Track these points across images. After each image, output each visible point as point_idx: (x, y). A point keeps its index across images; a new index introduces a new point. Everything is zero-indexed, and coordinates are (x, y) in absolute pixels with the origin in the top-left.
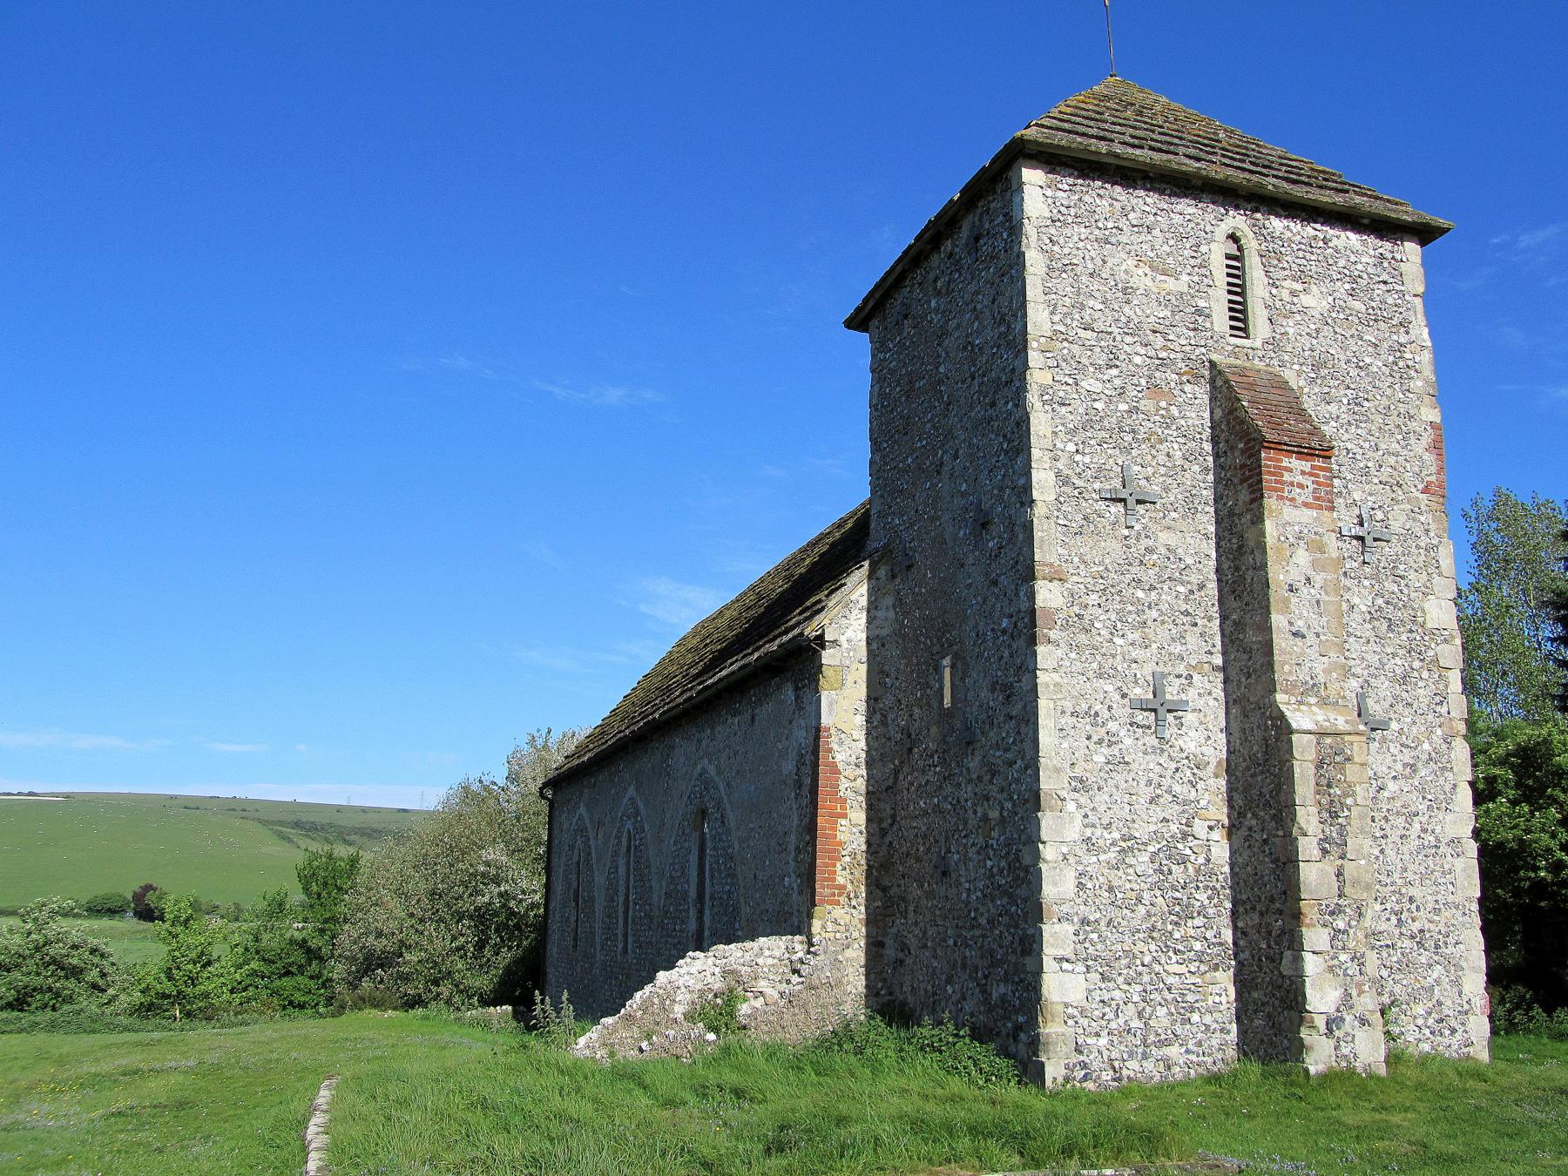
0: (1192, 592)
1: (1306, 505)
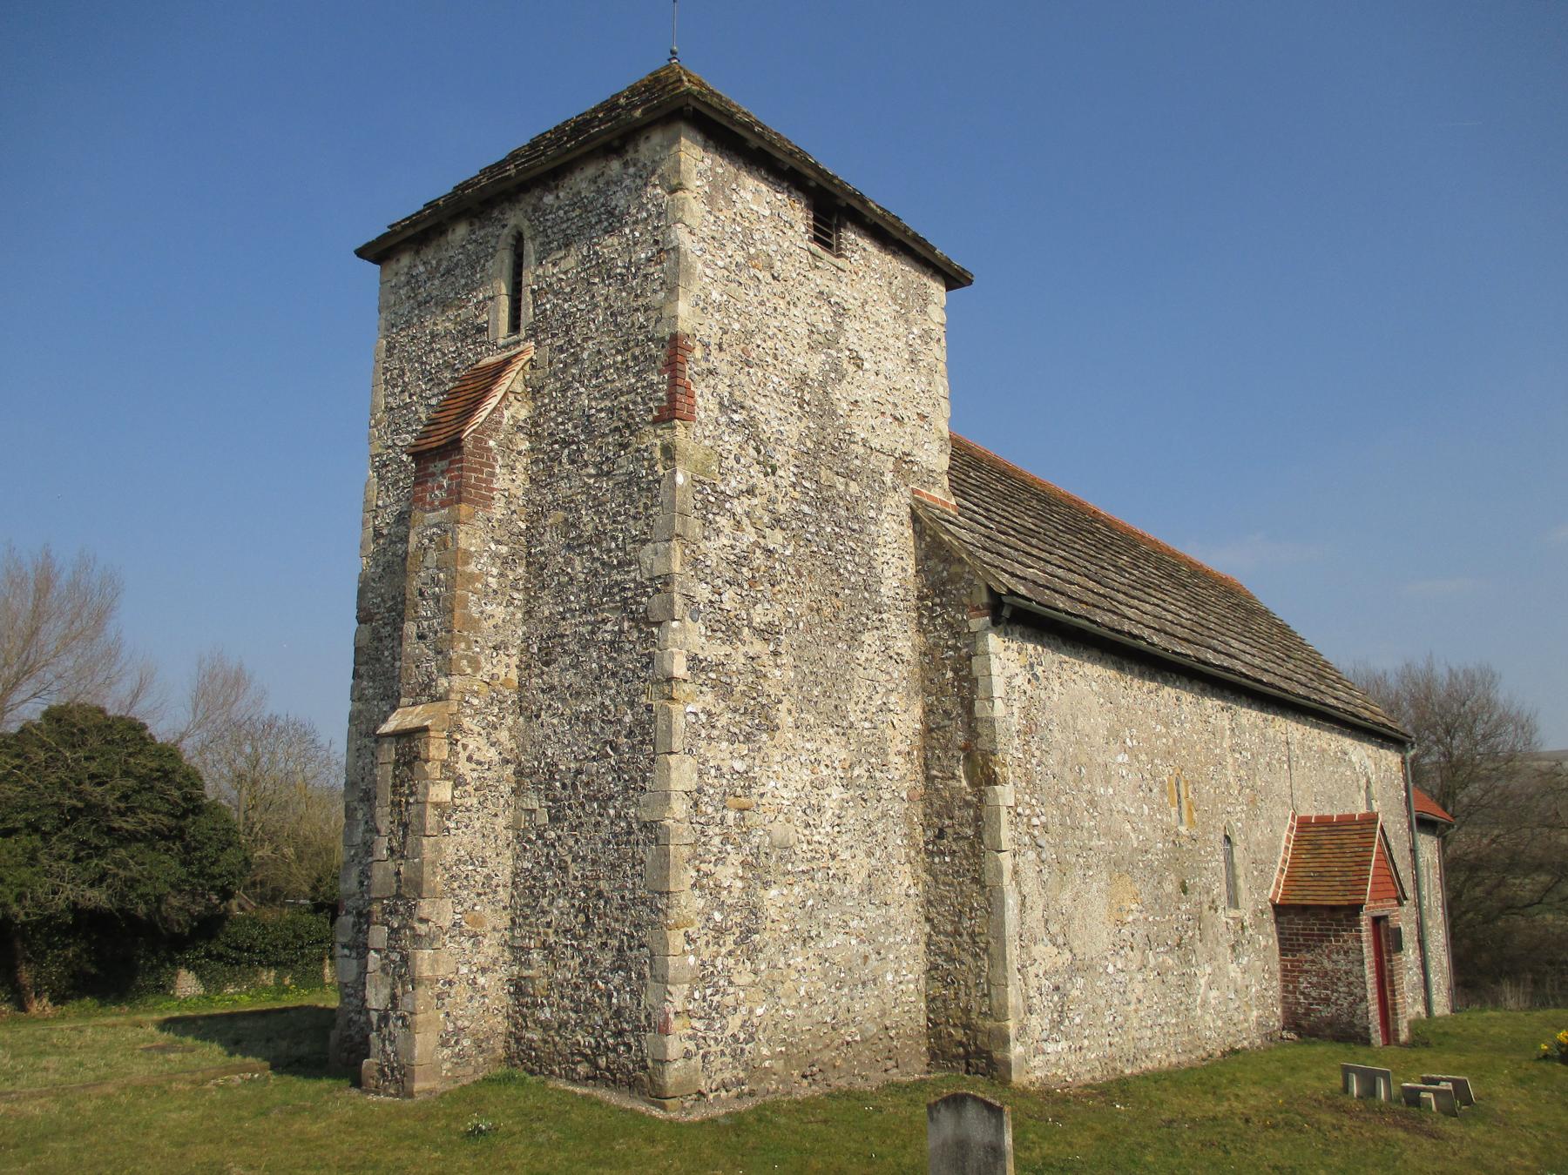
1: (443, 505)
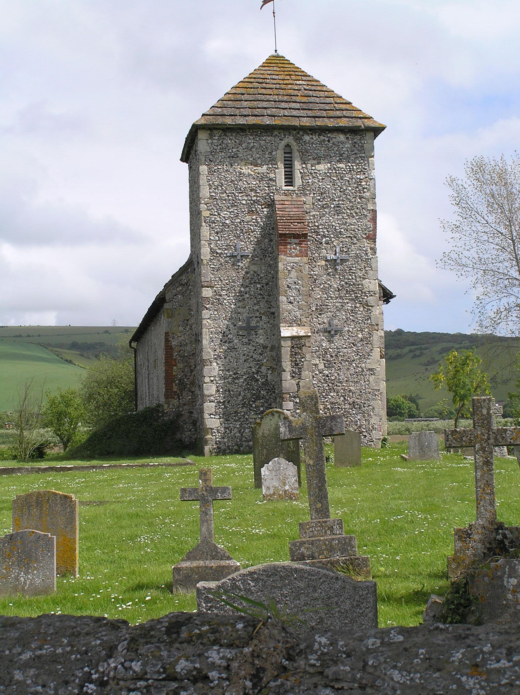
0: (263, 286)
1: (297, 256)
